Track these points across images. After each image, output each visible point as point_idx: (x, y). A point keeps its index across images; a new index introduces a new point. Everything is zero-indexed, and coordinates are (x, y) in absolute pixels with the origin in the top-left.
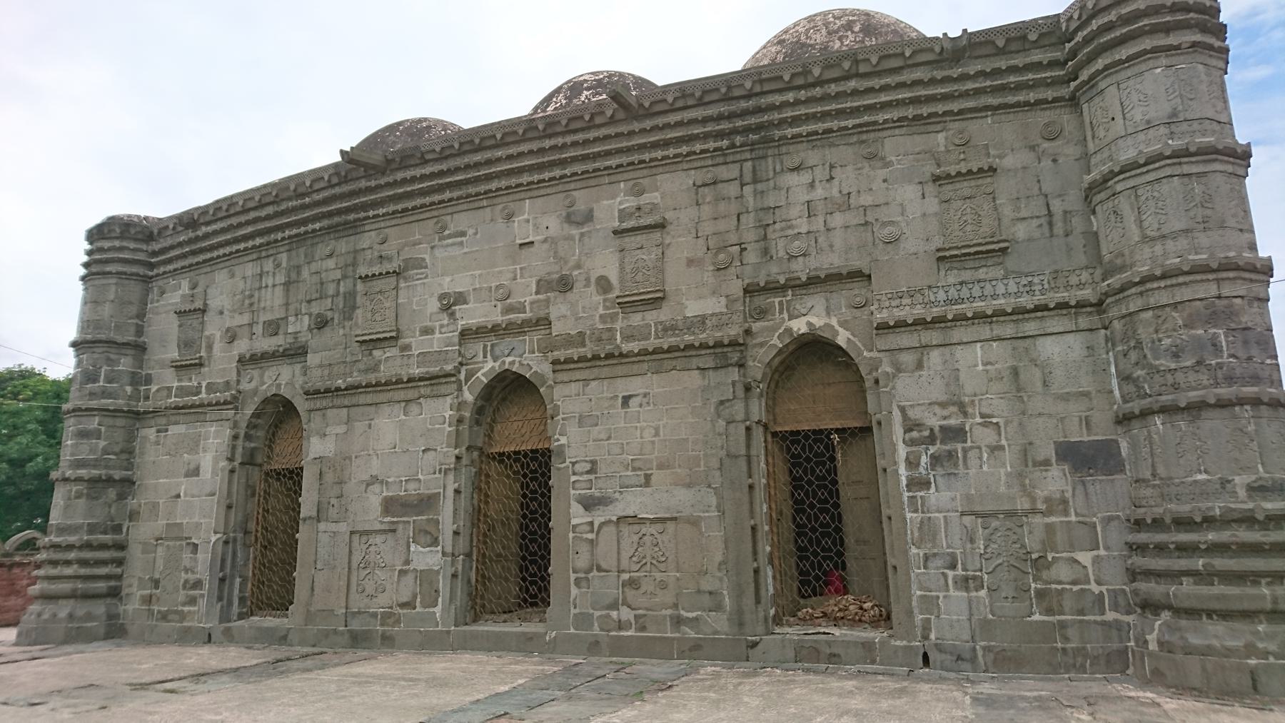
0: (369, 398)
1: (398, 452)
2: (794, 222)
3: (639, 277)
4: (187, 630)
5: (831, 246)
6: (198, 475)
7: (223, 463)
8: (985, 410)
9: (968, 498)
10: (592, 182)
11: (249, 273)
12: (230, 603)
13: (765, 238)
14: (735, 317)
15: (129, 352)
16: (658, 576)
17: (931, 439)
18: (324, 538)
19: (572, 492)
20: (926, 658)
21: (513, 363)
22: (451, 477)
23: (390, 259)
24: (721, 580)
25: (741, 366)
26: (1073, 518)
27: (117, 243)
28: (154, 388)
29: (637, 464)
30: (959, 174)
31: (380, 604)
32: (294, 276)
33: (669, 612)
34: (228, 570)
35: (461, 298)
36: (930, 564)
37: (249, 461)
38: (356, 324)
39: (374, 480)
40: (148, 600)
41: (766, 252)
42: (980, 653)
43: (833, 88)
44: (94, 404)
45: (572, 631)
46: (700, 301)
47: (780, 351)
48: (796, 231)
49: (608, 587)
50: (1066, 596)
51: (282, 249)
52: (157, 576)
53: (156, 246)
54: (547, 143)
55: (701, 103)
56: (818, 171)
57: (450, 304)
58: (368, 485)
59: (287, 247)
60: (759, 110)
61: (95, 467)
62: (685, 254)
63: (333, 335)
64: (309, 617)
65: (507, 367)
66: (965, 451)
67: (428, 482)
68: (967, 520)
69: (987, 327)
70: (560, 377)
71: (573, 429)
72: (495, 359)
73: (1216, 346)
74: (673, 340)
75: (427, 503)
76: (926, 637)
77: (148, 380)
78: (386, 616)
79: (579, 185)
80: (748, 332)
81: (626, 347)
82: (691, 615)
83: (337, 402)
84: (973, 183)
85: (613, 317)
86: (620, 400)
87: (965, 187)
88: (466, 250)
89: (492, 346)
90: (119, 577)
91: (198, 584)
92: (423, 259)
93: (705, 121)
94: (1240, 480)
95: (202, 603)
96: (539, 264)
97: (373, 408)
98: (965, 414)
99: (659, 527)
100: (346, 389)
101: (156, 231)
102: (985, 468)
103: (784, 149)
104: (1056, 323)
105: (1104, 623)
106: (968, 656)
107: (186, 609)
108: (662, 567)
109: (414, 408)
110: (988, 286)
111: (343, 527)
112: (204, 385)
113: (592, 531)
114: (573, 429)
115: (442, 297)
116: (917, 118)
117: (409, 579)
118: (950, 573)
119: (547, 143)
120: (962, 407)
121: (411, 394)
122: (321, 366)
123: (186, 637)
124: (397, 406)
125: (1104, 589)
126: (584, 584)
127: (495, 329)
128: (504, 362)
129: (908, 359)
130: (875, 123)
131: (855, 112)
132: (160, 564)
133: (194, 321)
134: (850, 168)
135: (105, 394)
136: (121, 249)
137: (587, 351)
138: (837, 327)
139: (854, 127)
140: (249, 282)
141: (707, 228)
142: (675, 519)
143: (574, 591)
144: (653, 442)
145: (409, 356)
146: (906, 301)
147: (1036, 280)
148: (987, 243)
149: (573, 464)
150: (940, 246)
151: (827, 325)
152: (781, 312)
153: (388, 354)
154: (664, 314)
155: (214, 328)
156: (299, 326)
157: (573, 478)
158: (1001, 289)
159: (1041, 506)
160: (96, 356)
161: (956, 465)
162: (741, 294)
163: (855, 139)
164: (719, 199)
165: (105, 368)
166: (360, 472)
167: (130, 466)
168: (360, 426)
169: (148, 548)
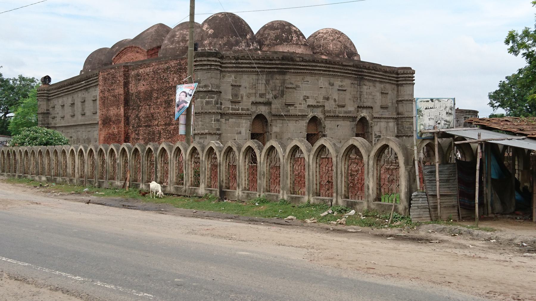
23: (292, 84)
35: (308, 98)
41: (360, 100)
46: (351, 107)
54: (328, 66)
57: (306, 98)
70: (326, 119)
83: (280, 118)
85: (336, 108)
127: (315, 106)
141: (352, 93)
168: (285, 125)
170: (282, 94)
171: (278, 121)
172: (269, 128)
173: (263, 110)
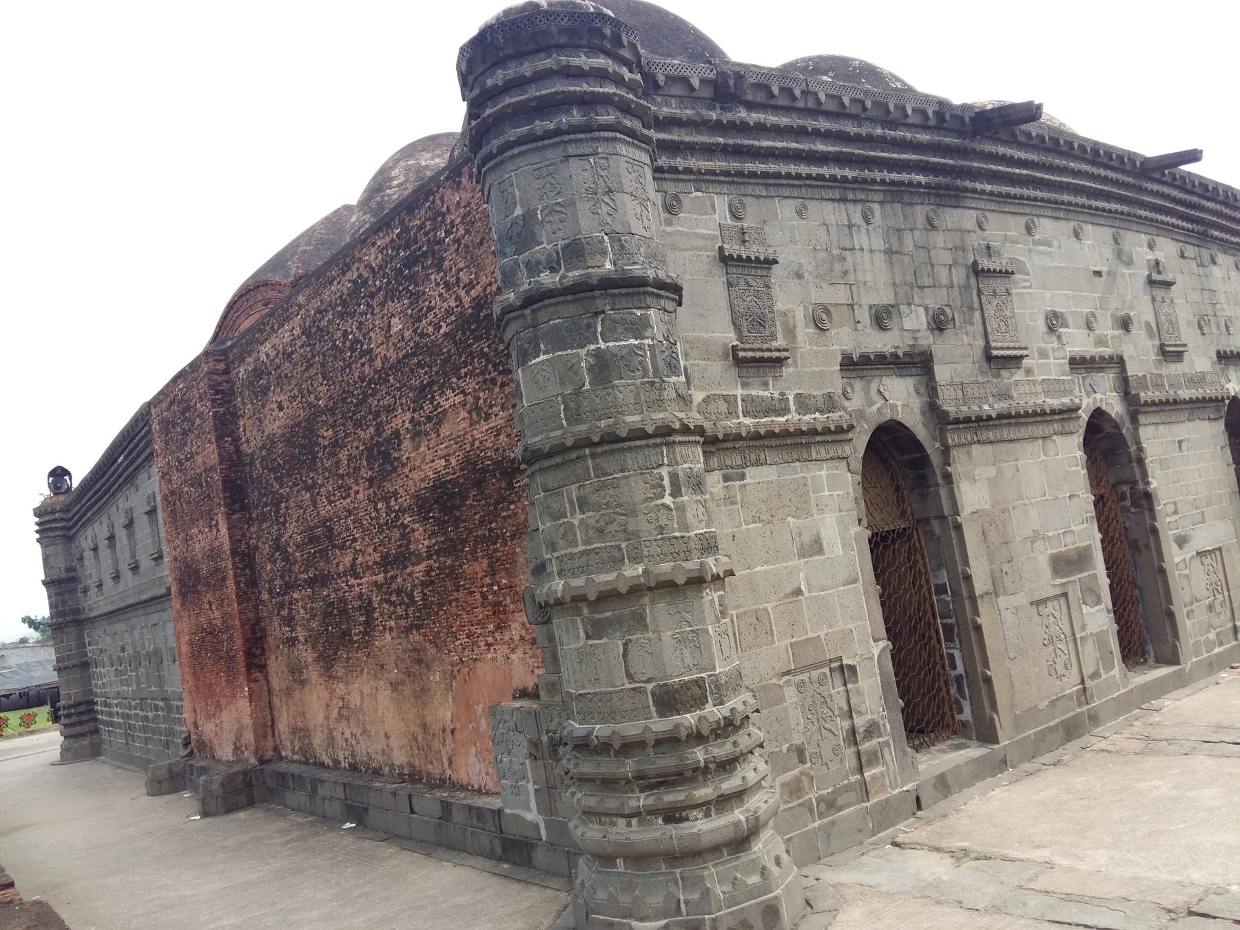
6: (820, 551)
7: (855, 529)
18: (1008, 617)
21: (1101, 400)
32: (895, 242)
39: (1036, 537)
51: (876, 198)
57: (1054, 322)
58: (1032, 543)
65: (1099, 405)
111: (1022, 599)
112: (791, 398)
122: (951, 384)
124: (1036, 443)
145: (1034, 382)
171: (976, 449)
172: (943, 493)
173: (899, 398)
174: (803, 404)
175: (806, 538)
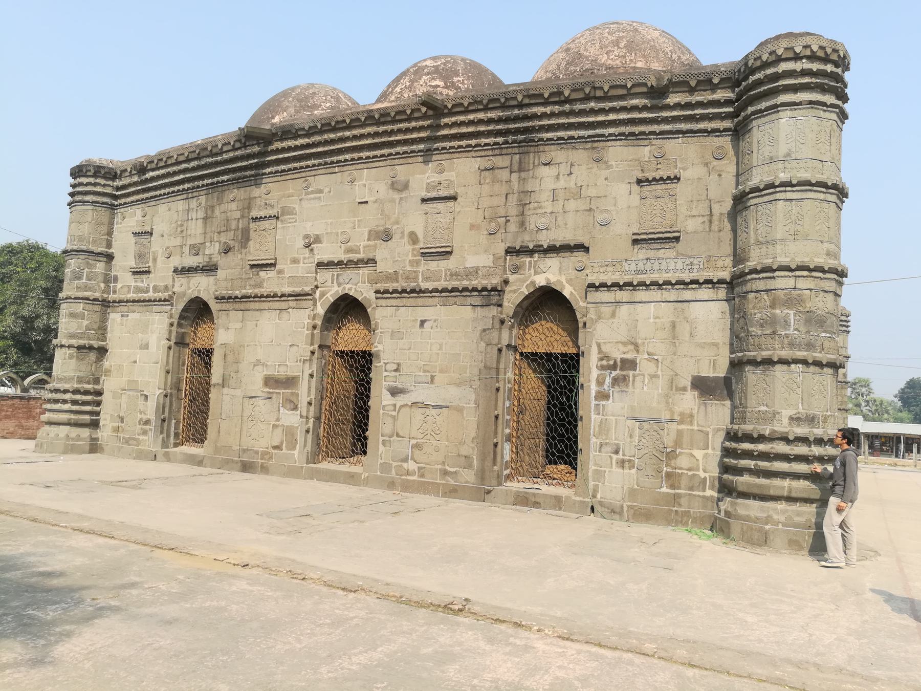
0: (257, 305)
1: (270, 346)
2: (543, 204)
3: (438, 235)
4: (141, 452)
5: (566, 224)
8: (650, 350)
9: (632, 408)
10: (410, 160)
11: (180, 208)
12: (168, 436)
13: (523, 214)
14: (498, 270)
15: (102, 259)
16: (435, 443)
17: (614, 367)
18: (226, 399)
19: (384, 383)
20: (592, 509)
21: (350, 289)
22: (307, 365)
23: (272, 206)
24: (473, 448)
25: (500, 306)
26: (695, 428)
27: (92, 180)
28: (119, 285)
29: (427, 368)
30: (654, 179)
31: (262, 444)
32: (209, 212)
33: (440, 467)
34: (166, 414)
35: (318, 240)
36: (602, 449)
37: (181, 342)
38: (249, 252)
39: (258, 363)
40: (117, 430)
41: (522, 224)
42: (625, 509)
43: (578, 107)
44: (80, 294)
45: (379, 473)
46: (477, 257)
47: (527, 297)
48: (544, 211)
49: (403, 447)
50: (684, 477)
51: (202, 193)
52: (122, 414)
53: (118, 183)
54: (382, 129)
55: (486, 109)
56: (563, 166)
58: (255, 366)
59: (205, 192)
60: (526, 118)
61: (81, 338)
62: (469, 221)
63: (234, 258)
64: (217, 450)
66: (634, 376)
67: (292, 368)
68: (630, 422)
69: (659, 292)
70: (383, 302)
71: (387, 339)
72: (339, 285)
73: (786, 324)
74: (455, 284)
75: (290, 382)
76: (594, 496)
77: (116, 279)
78: (264, 454)
79: (401, 161)
80: (506, 282)
81: (424, 285)
82: (452, 470)
83: (237, 306)
84: (664, 186)
85: (418, 263)
86: (419, 323)
87: (658, 188)
88: (322, 203)
89: (338, 275)
90: (98, 414)
91: (147, 422)
92: (294, 208)
93: (490, 121)
94: (786, 413)
95: (151, 434)
96: (372, 218)
97: (258, 312)
98: (638, 351)
99: (438, 411)
100: (242, 298)
101: (119, 172)
102: (645, 389)
103: (541, 148)
104: (705, 293)
105: (704, 497)
106: (618, 510)
107: (141, 437)
108: (437, 437)
109: (284, 315)
110: (664, 262)
111: (239, 393)
113: (395, 410)
114: (387, 339)
115: (306, 236)
116: (632, 134)
117: (279, 430)
118: (615, 457)
119: (382, 129)
120: (636, 346)
121: (283, 305)
122: (226, 280)
123: (141, 456)
124: (274, 312)
125: (707, 475)
126: (388, 444)
127: (340, 263)
128: (344, 288)
129: (607, 310)
130: (603, 135)
131: (591, 126)
132: (124, 406)
133: (144, 240)
134: (584, 167)
135: (86, 288)
136: (95, 185)
137: (398, 286)
138: (565, 283)
139: (589, 137)
140: (180, 214)
141: (486, 202)
142: (447, 407)
143: (381, 448)
144: (438, 354)
145: (283, 278)
146: (610, 269)
147: (696, 262)
148: (666, 232)
149: (386, 364)
150: (636, 231)
151: (558, 281)
152: (529, 269)
153: (269, 275)
154: (451, 264)
155: (157, 245)
156: (213, 250)
157: (385, 374)
158: (672, 266)
159: (677, 418)
160: (80, 261)
161: (627, 385)
162: (503, 253)
163: (589, 145)
164: (495, 181)
165: (86, 270)
166: (249, 357)
167: (104, 339)
168: (250, 325)
169: (116, 396)
170: (245, 238)
174: (156, 289)
175: (144, 342)
